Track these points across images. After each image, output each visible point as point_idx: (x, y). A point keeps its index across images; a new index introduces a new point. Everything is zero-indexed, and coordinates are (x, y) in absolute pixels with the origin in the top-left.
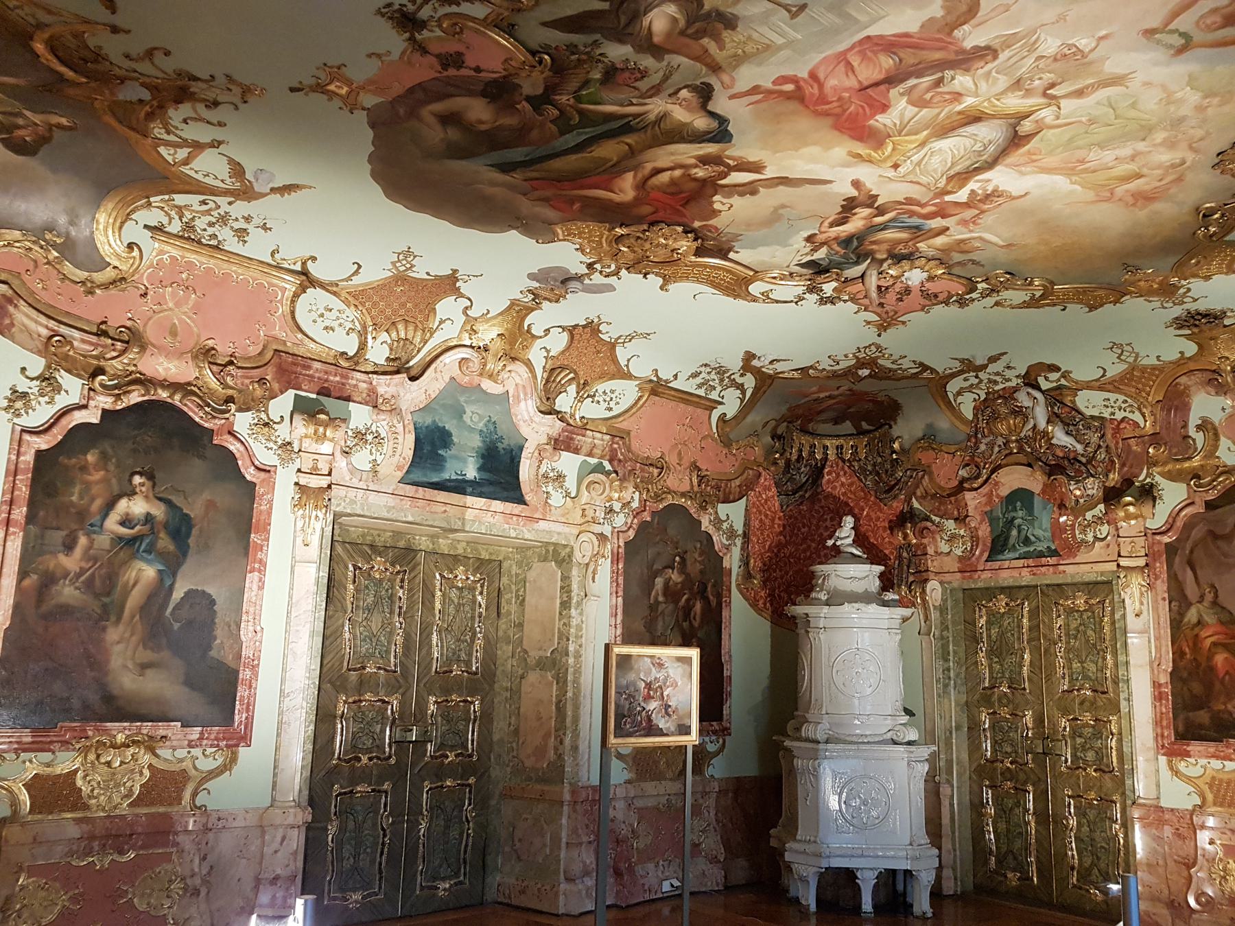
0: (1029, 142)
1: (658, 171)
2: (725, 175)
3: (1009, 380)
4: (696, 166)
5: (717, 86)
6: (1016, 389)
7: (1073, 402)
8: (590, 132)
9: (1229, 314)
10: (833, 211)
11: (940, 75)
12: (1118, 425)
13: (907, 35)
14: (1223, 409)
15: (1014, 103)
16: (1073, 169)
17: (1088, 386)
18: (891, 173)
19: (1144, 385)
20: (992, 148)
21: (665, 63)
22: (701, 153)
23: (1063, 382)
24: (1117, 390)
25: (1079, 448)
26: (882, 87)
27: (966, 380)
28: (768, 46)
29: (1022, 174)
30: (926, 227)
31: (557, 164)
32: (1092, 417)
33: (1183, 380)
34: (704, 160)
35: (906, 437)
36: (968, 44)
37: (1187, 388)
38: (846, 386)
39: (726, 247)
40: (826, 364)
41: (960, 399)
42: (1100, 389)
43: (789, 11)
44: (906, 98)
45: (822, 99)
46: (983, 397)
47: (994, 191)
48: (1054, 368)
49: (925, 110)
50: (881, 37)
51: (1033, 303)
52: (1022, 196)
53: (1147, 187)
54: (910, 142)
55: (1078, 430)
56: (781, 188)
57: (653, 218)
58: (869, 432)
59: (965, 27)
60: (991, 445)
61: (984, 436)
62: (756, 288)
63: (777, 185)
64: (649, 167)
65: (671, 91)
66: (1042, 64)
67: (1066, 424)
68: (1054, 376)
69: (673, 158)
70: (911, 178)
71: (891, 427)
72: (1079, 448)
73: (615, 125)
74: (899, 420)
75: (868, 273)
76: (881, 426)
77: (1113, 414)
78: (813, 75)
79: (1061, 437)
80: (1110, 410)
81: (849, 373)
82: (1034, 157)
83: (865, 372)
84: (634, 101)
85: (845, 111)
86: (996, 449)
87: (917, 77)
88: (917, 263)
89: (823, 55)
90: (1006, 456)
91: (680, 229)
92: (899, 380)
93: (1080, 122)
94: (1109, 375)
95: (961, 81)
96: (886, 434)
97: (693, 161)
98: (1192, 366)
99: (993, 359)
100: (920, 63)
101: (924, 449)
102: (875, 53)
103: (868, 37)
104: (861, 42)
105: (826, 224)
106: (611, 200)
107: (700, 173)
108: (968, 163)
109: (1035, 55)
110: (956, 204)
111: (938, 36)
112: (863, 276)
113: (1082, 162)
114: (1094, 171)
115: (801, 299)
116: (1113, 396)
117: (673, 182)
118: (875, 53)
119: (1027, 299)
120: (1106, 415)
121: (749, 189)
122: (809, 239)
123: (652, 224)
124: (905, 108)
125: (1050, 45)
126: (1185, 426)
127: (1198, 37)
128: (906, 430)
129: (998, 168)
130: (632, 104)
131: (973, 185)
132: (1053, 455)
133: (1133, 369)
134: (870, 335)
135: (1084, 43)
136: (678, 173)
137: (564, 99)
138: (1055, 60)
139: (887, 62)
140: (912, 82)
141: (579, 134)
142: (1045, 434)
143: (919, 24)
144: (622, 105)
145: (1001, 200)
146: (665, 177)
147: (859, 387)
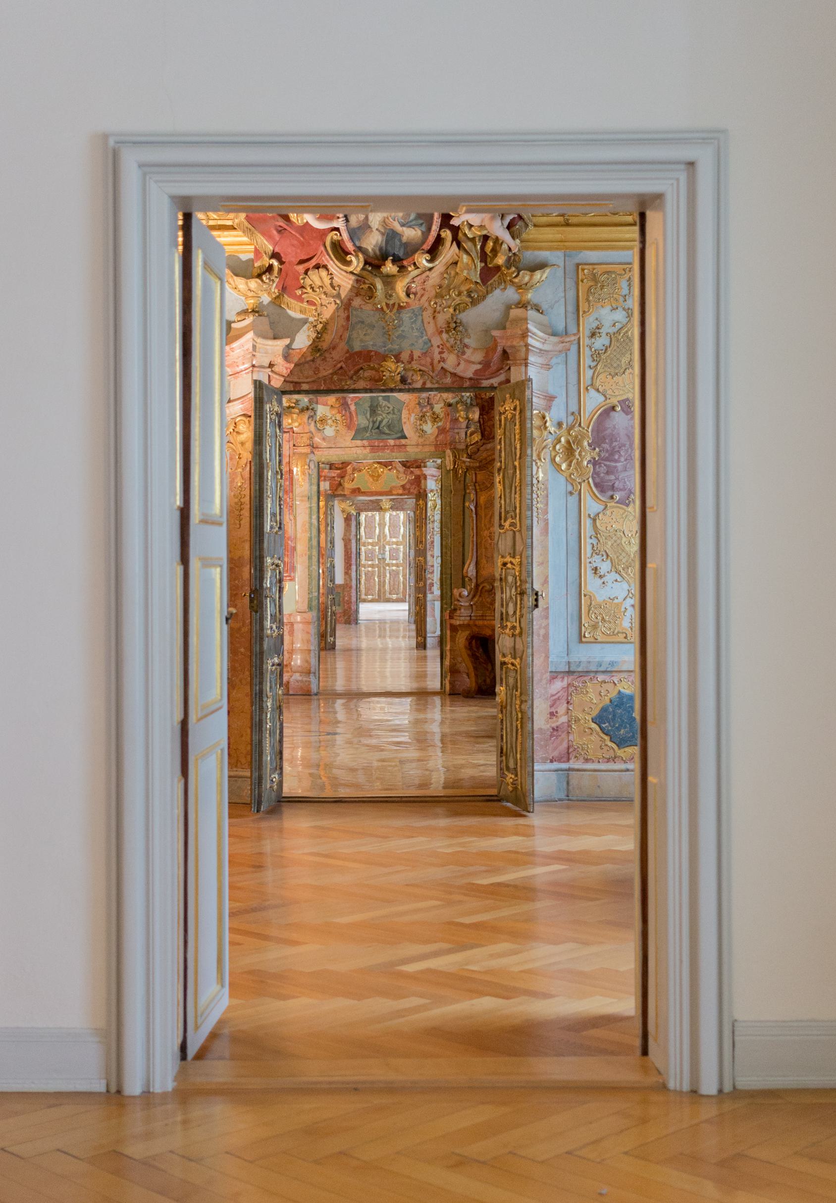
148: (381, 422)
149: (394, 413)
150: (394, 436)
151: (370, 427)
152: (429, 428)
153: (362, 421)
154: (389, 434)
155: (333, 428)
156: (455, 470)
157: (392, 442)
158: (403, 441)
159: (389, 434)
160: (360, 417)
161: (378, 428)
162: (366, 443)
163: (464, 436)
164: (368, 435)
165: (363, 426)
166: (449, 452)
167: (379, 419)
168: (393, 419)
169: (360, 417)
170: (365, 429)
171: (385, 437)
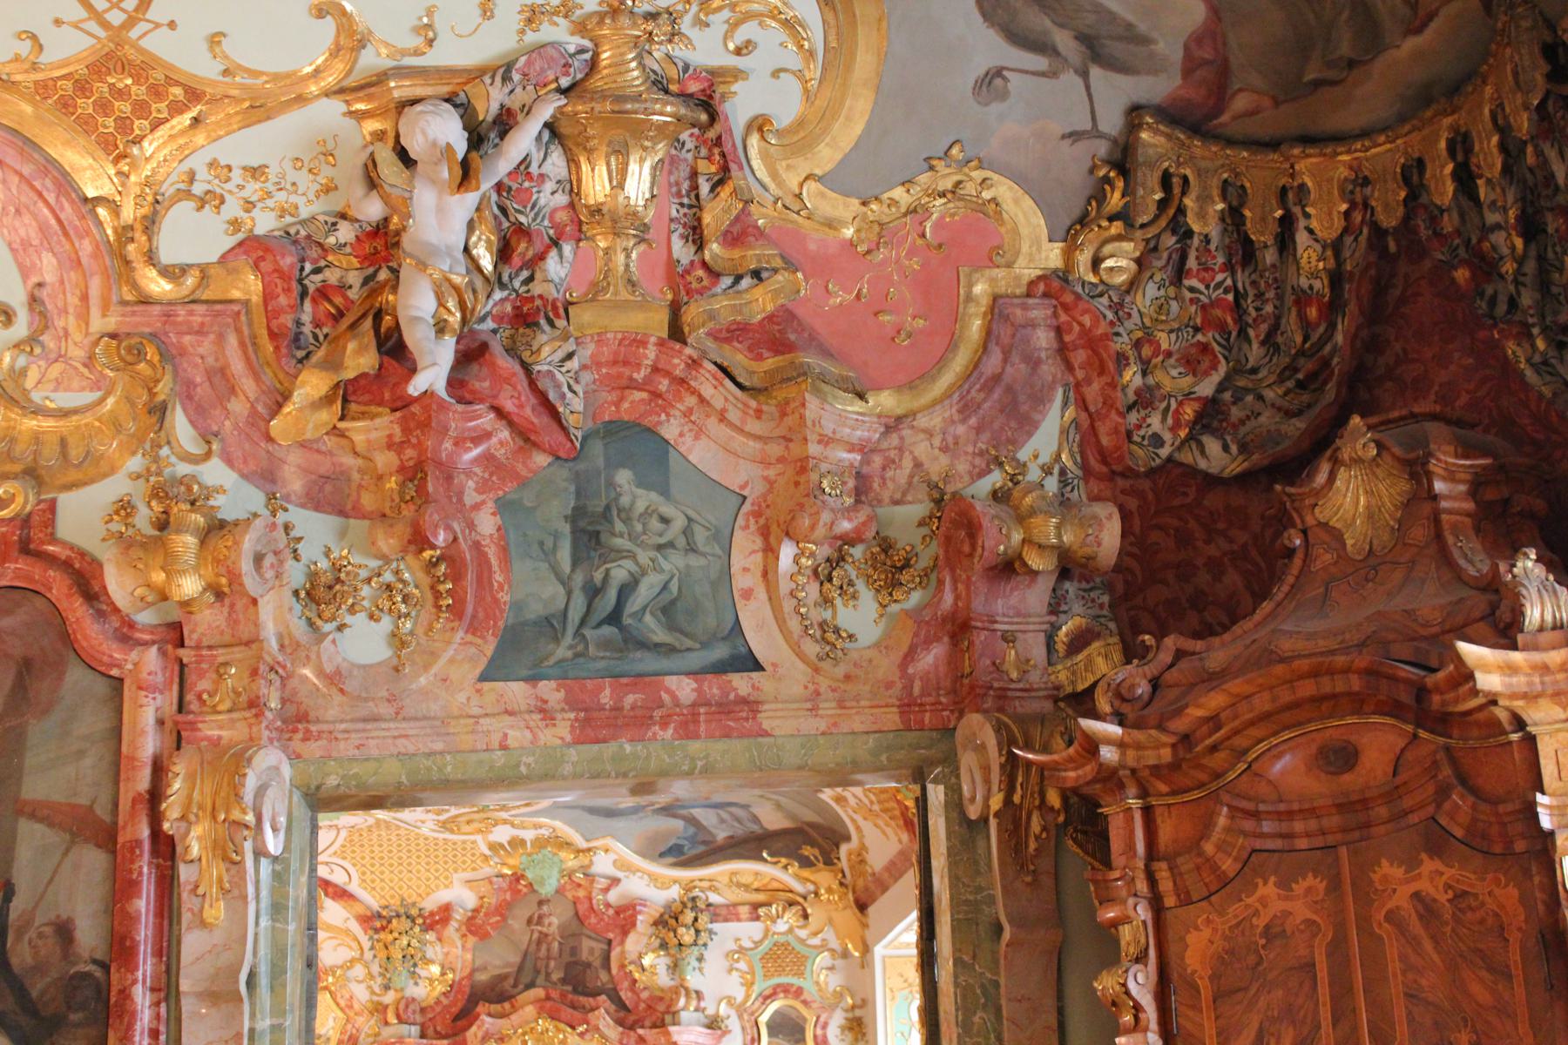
148: (626, 590)
149: (691, 549)
150: (697, 659)
151: (575, 615)
152: (862, 616)
153: (533, 586)
154: (671, 650)
155: (386, 623)
156: (1013, 818)
157: (684, 688)
158: (741, 683)
159: (671, 650)
160: (521, 568)
161: (614, 618)
162: (549, 690)
163: (1038, 653)
164: (562, 652)
165: (535, 610)
166: (979, 729)
167: (620, 573)
168: (685, 575)
169: (521, 568)
170: (551, 626)
171: (647, 662)
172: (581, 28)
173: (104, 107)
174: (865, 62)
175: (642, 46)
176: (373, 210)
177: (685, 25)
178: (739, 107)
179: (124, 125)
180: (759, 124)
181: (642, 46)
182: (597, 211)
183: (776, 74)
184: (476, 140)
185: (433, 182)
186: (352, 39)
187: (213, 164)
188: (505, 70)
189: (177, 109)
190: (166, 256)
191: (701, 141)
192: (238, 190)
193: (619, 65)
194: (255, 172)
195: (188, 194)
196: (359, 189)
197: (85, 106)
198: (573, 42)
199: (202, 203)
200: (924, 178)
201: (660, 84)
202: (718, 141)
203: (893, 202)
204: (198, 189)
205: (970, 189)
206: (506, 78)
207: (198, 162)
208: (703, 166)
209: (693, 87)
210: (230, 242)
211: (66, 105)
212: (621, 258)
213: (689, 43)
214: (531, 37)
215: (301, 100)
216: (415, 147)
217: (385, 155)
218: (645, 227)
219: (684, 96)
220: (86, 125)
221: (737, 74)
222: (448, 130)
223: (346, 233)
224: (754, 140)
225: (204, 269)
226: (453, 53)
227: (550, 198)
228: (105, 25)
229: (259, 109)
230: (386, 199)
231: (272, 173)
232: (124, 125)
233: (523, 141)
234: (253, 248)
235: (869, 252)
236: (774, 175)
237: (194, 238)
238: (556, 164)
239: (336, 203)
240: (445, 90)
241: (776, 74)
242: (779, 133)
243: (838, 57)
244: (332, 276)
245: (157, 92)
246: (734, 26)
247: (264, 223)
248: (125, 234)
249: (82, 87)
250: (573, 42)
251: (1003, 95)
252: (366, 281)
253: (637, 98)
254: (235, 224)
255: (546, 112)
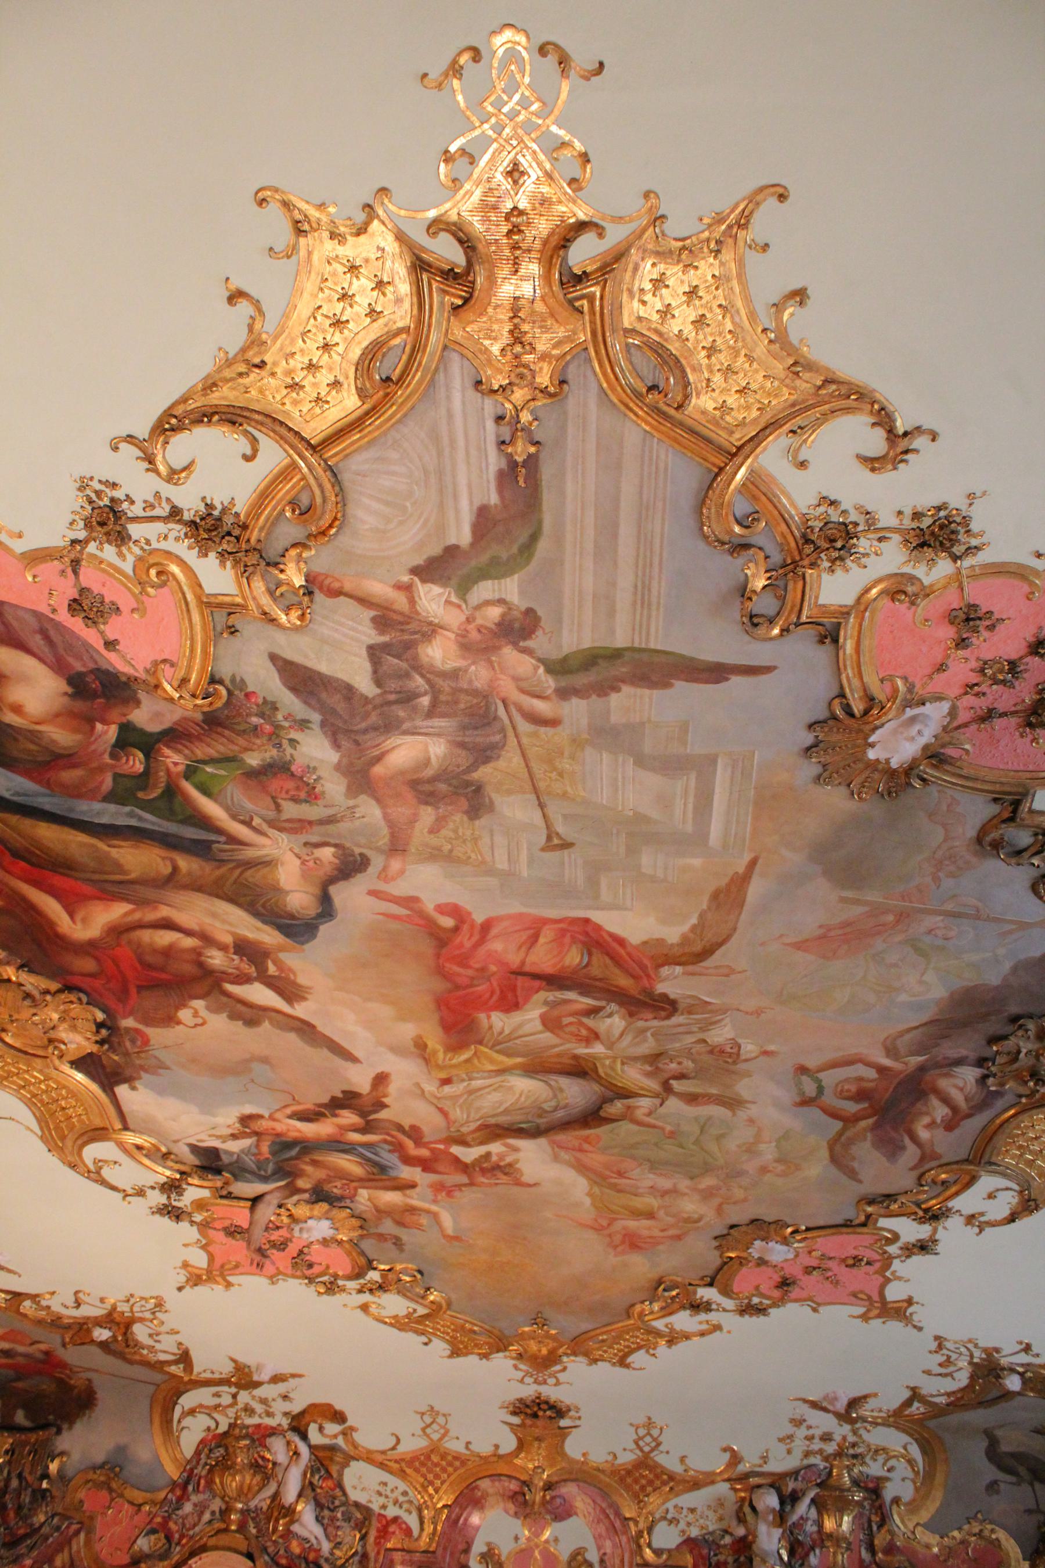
0: (599, 1126)
1: (168, 925)
2: (243, 979)
3: (269, 1414)
4: (223, 948)
5: (372, 870)
6: (273, 1432)
7: (341, 1474)
8: (150, 821)
9: (572, 1413)
10: (315, 1096)
11: (603, 1003)
12: (387, 1526)
13: (621, 942)
14: (516, 1538)
15: (633, 1076)
16: (605, 1178)
17: (370, 1458)
18: (430, 1087)
19: (437, 1477)
20: (560, 1114)
21: (351, 803)
22: (251, 935)
23: (340, 1441)
24: (402, 1474)
25: (326, 1547)
26: (537, 983)
27: (217, 1395)
28: (483, 862)
29: (556, 1158)
30: (393, 1173)
31: (47, 833)
32: (357, 1505)
33: (485, 1484)
34: (243, 948)
35: (76, 1456)
36: (661, 988)
37: (485, 1495)
38: (51, 1341)
39: (128, 1072)
40: (60, 1305)
41: (188, 1421)
42: (382, 1466)
43: (549, 838)
44: (544, 1009)
45: (463, 961)
46: (223, 1428)
47: (510, 1165)
48: (339, 1417)
49: (548, 1034)
50: (598, 928)
51: (400, 1324)
52: (529, 1185)
53: (645, 1233)
54: (492, 1061)
55: (333, 1519)
56: (292, 1036)
57: (77, 981)
58: (21, 1429)
59: (678, 969)
60: (200, 1509)
61: (197, 1490)
62: (92, 1152)
63: (292, 1029)
64: (164, 912)
65: (314, 839)
66: (700, 1047)
67: (319, 1505)
68: (332, 1428)
69: (208, 920)
70: (447, 1105)
71: (59, 1432)
72: (326, 1547)
73: (191, 833)
74: (78, 1426)
75: (268, 1198)
76: (45, 1426)
77: (384, 1507)
78: (486, 927)
79: (308, 1524)
80: (382, 1500)
81: (80, 1330)
82: (586, 1146)
83: (102, 1334)
84: (257, 821)
85: (472, 986)
86: (207, 1517)
87: (581, 994)
88: (335, 1212)
89: (524, 910)
90: (219, 1531)
91: (100, 1016)
92: (131, 1362)
93: (663, 1129)
94: (401, 1448)
95: (614, 1022)
96: (46, 1443)
97: (228, 940)
98: (502, 1468)
99: (276, 1379)
100: (600, 980)
101: (99, 1485)
102: (574, 940)
103: (587, 921)
104: (574, 921)
105: (288, 1111)
106: (51, 924)
107: (216, 959)
108: (518, 1118)
109: (701, 1036)
110: (457, 1160)
111: (646, 962)
112: (256, 1200)
113: (620, 1174)
114: (620, 1191)
115: (140, 1193)
116: (393, 1481)
117: (168, 952)
118: (574, 940)
119: (403, 1312)
120: (375, 1507)
121: (251, 1015)
122: (246, 1120)
123: (68, 988)
124: (531, 1020)
125: (721, 1035)
126: (467, 1551)
127: (829, 1099)
128: (80, 1445)
129: (542, 1141)
130: (248, 823)
131: (496, 1148)
132: (287, 1550)
133: (432, 1451)
134: (165, 1281)
135: (749, 1048)
136: (189, 942)
137: (173, 759)
138: (711, 1052)
139: (574, 957)
140: (571, 995)
141: (131, 815)
142: (290, 1512)
143: (645, 938)
144: (234, 817)
145: (504, 1179)
146: (165, 938)
147: (72, 1356)
172: (826, 1459)
173: (636, 1481)
174: (939, 1478)
175: (849, 1469)
176: (741, 1531)
177: (868, 1459)
178: (889, 1492)
179: (643, 1488)
180: (896, 1501)
181: (849, 1469)
182: (830, 1536)
183: (903, 1480)
184: (782, 1503)
185: (766, 1521)
186: (735, 1459)
187: (675, 1507)
188: (795, 1474)
189: (664, 1483)
190: (655, 1545)
191: (872, 1506)
192: (685, 1517)
193: (840, 1476)
194: (692, 1510)
195: (664, 1518)
196: (734, 1523)
197: (629, 1480)
198: (822, 1465)
199: (671, 1522)
200: (966, 1527)
201: (855, 1482)
202: (880, 1507)
203: (954, 1538)
204: (669, 1516)
205: (986, 1533)
206: (796, 1479)
207: (670, 1505)
208: (874, 1518)
209: (871, 1485)
210: (680, 1540)
211: (622, 1480)
212: (840, 1557)
213: (868, 1465)
214: (806, 1462)
215: (713, 1482)
216: (760, 1506)
217: (747, 1509)
218: (849, 1544)
219: (866, 1489)
220: (628, 1488)
221: (888, 1479)
222: (771, 1500)
223: (727, 1540)
224: (894, 1507)
225: (669, 1551)
226: (776, 1466)
227: (810, 1528)
228: (642, 1450)
229: (695, 1485)
230: (747, 1529)
231: (699, 1511)
232: (643, 1488)
233: (803, 1508)
234: (690, 1543)
235: (945, 1561)
236: (903, 1522)
237: (666, 1537)
238: (813, 1513)
239: (724, 1525)
240: (768, 1481)
241: (903, 1480)
242: (906, 1505)
243: (929, 1476)
244: (722, 1558)
245: (657, 1477)
246: (887, 1460)
247: (694, 1532)
248: (640, 1534)
249: (629, 1473)
250: (822, 1465)
251: (998, 1492)
252: (736, 1561)
253: (849, 1490)
254: (683, 1532)
255: (812, 1494)
